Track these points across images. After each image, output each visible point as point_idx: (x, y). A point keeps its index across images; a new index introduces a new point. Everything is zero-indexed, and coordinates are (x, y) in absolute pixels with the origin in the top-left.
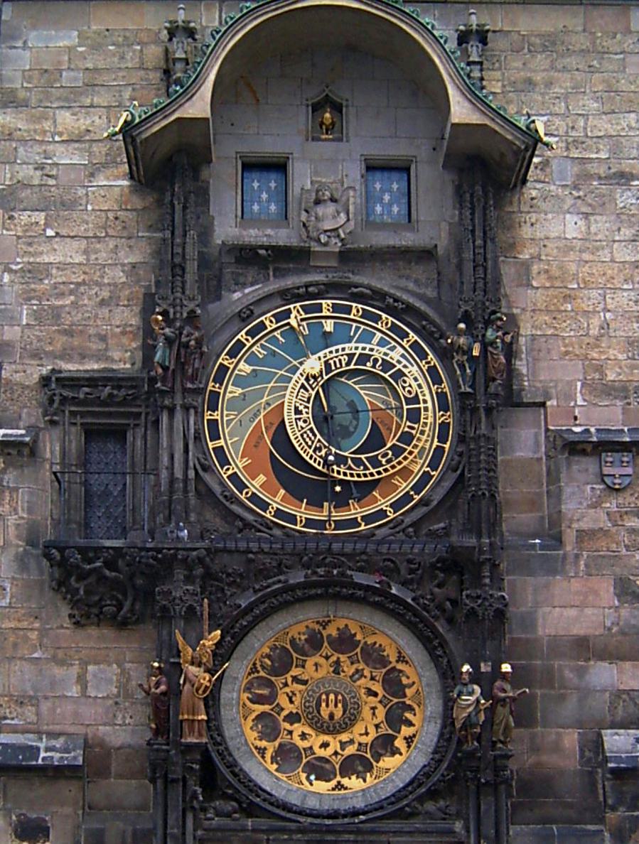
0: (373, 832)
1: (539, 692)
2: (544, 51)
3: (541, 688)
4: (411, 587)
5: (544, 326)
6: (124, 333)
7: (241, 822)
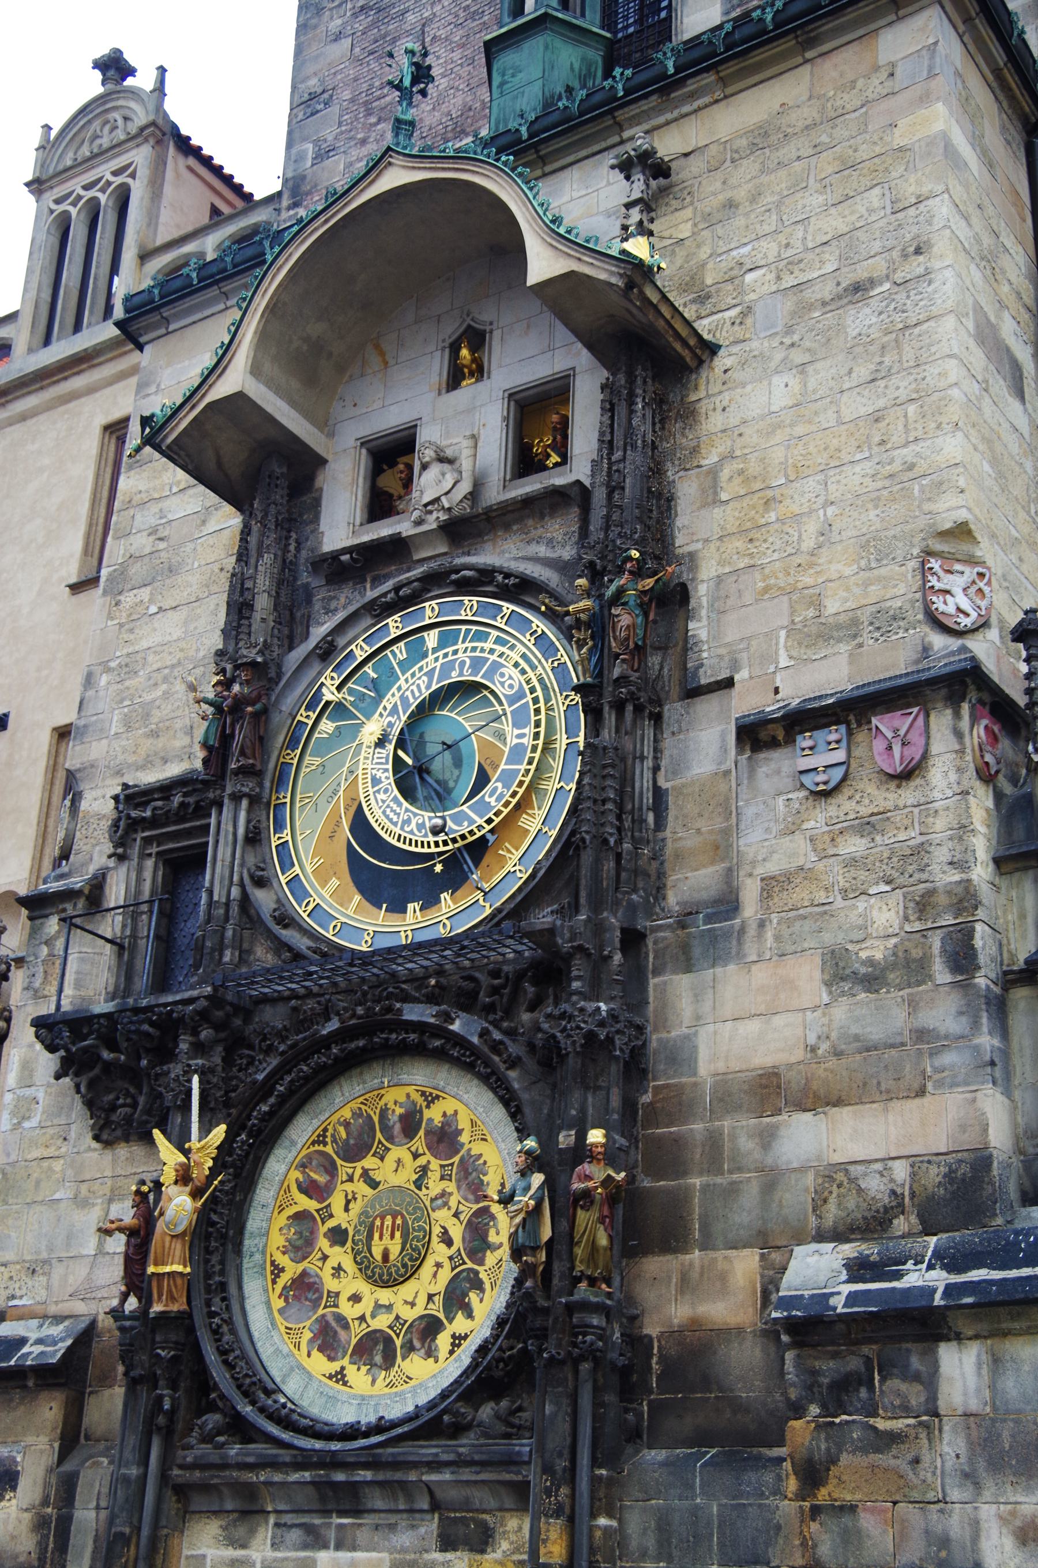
0: (396, 1465)
1: (697, 1182)
2: (752, 153)
3: (701, 1174)
5: (735, 557)
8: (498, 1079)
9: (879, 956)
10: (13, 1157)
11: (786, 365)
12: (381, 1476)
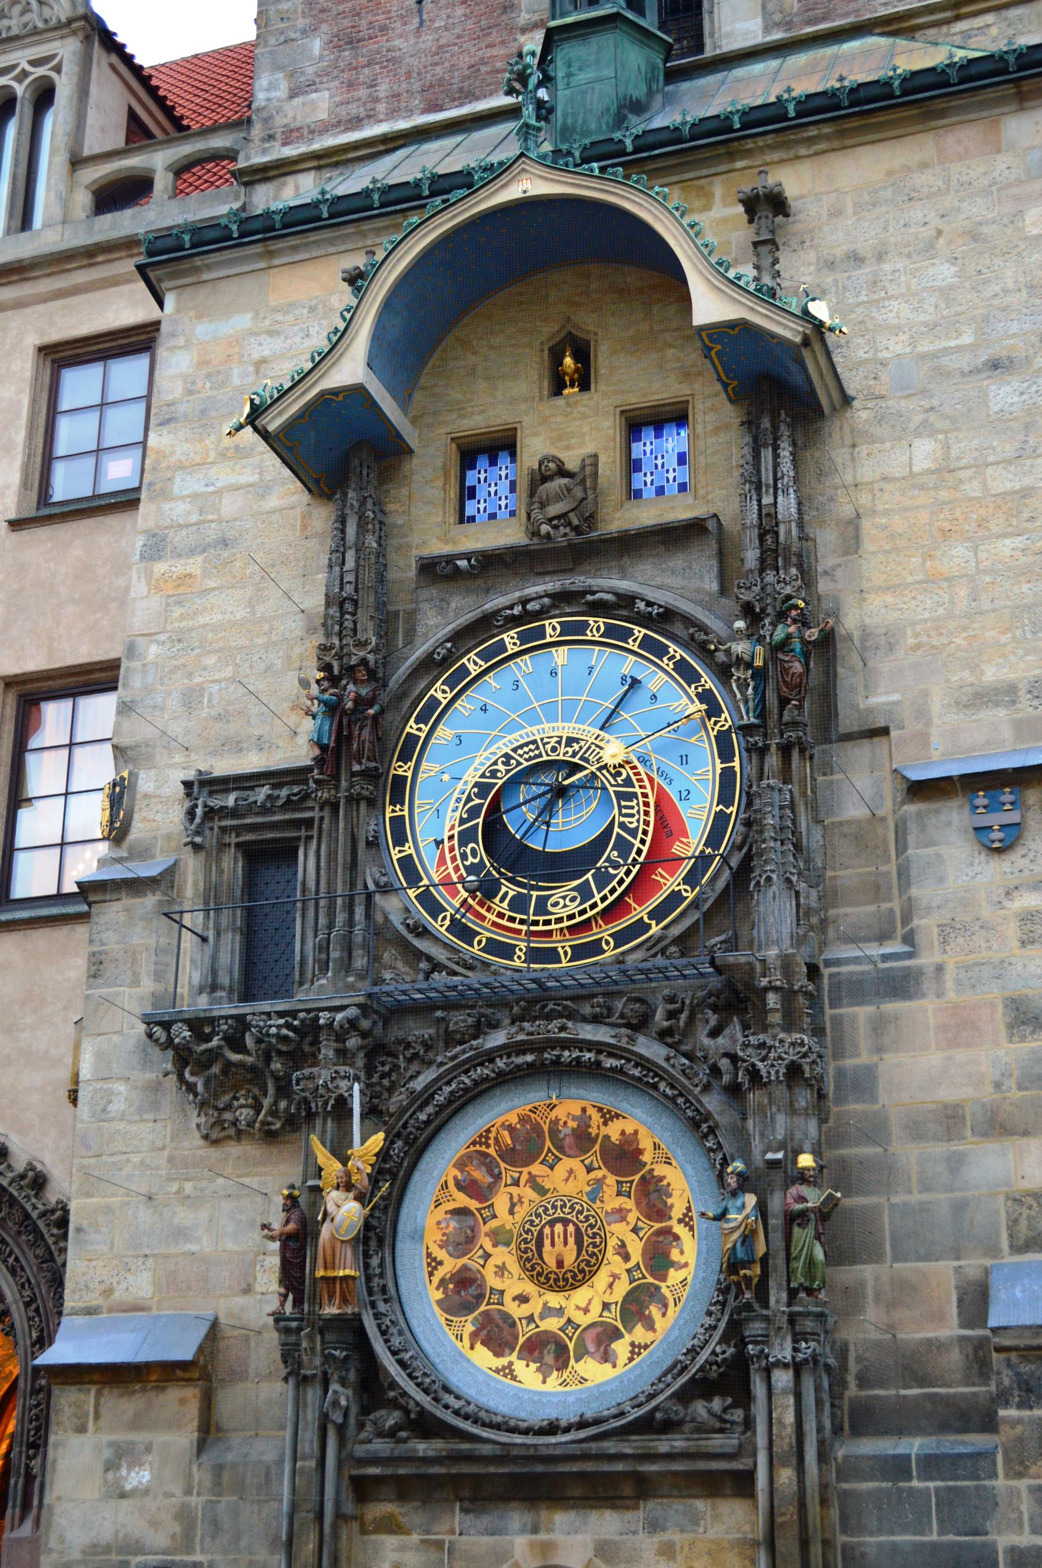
4: (669, 1040)
5: (883, 610)
6: (293, 709)
7: (411, 1445)
8: (687, 1101)
11: (926, 429)
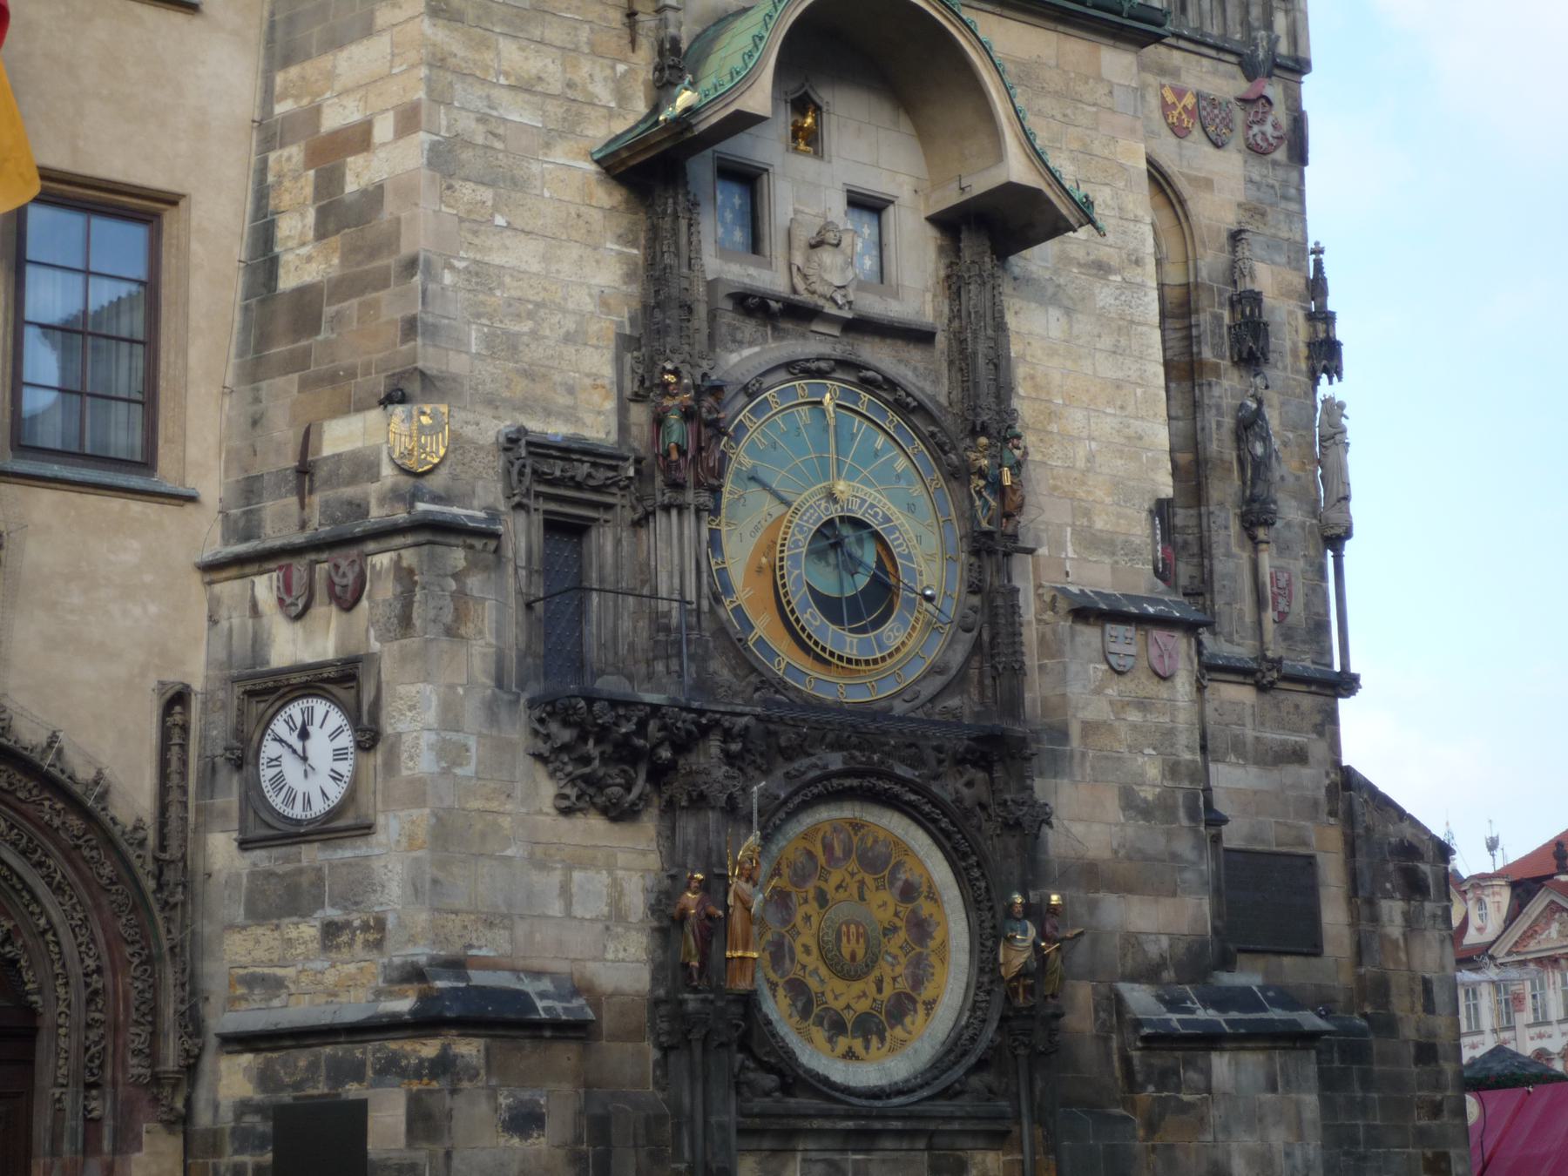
9: (1150, 798)
10: (447, 803)
12: (910, 1125)
